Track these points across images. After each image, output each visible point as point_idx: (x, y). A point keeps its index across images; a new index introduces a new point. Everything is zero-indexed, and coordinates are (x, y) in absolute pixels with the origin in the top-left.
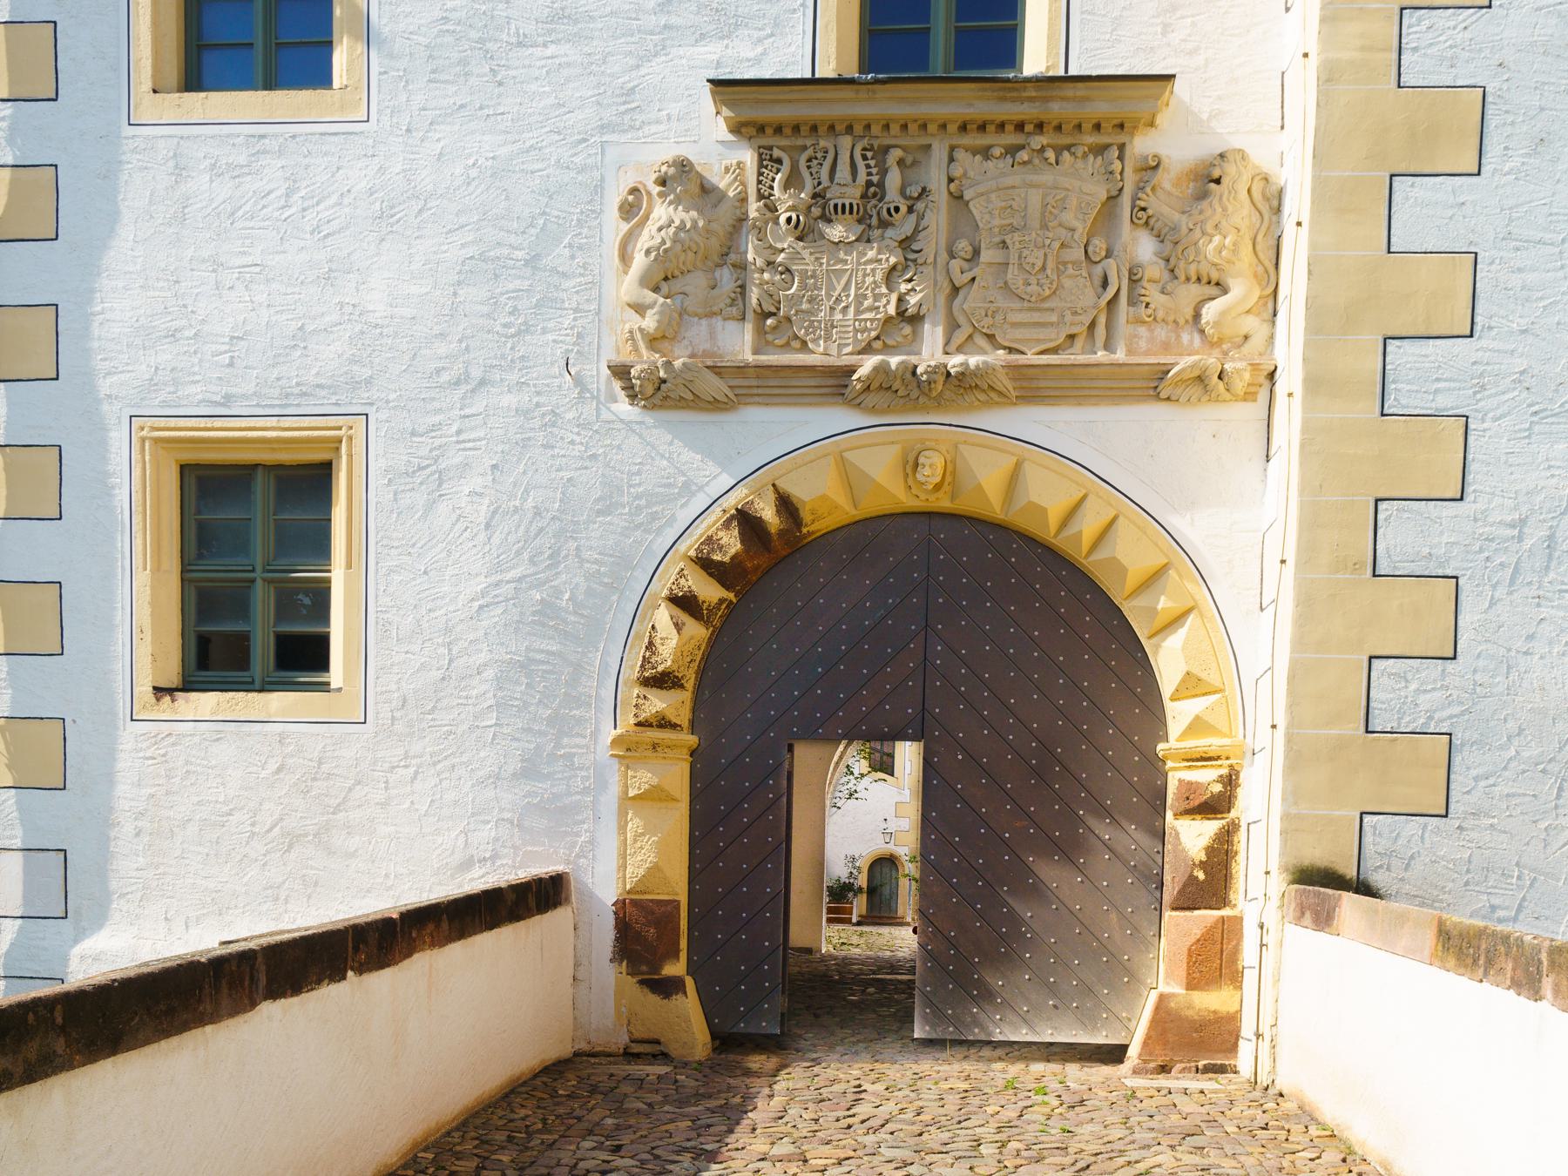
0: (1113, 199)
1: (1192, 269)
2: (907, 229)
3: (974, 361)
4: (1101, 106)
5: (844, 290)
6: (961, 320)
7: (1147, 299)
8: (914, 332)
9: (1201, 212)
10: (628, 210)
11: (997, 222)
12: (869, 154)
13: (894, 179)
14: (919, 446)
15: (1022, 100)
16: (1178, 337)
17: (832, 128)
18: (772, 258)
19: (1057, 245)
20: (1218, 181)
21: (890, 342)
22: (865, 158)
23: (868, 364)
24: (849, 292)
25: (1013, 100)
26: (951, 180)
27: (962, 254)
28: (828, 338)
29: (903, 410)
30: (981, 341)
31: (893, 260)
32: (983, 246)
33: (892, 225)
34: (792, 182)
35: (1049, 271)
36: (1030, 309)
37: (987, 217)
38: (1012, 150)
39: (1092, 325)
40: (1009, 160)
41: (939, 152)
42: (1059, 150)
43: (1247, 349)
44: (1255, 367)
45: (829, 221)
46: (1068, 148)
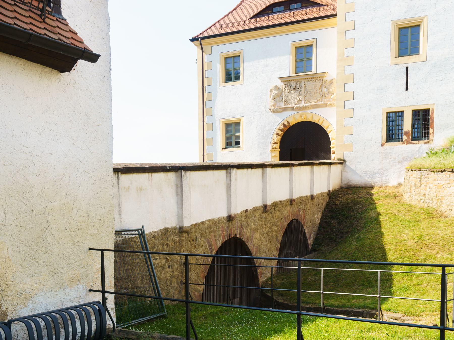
0: (322, 85)
10: (271, 91)
13: (298, 85)
34: (288, 87)
38: (311, 81)
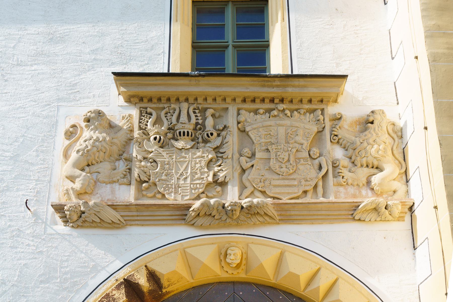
0: (320, 132)
1: (364, 161)
2: (218, 142)
3: (255, 201)
4: (312, 90)
5: (184, 170)
6: (247, 184)
7: (343, 174)
8: (223, 191)
9: (365, 136)
11: (263, 140)
12: (197, 111)
13: (210, 122)
14: (227, 245)
15: (273, 87)
16: (360, 192)
17: (178, 99)
18: (146, 156)
19: (294, 150)
20: (372, 123)
21: (210, 195)
22: (194, 112)
23: (197, 204)
24: (187, 174)
25: (269, 86)
26: (239, 123)
27: (246, 154)
28: (176, 193)
29: (219, 227)
30: (257, 193)
31: (210, 156)
32: (256, 150)
33: (210, 141)
34: (158, 121)
35: (291, 162)
36: (284, 179)
37: (258, 138)
38: (269, 111)
39: (316, 187)
40: (267, 115)
41: (232, 110)
42: (292, 111)
43: (396, 196)
44: (403, 204)
45: (177, 140)
46: (297, 110)
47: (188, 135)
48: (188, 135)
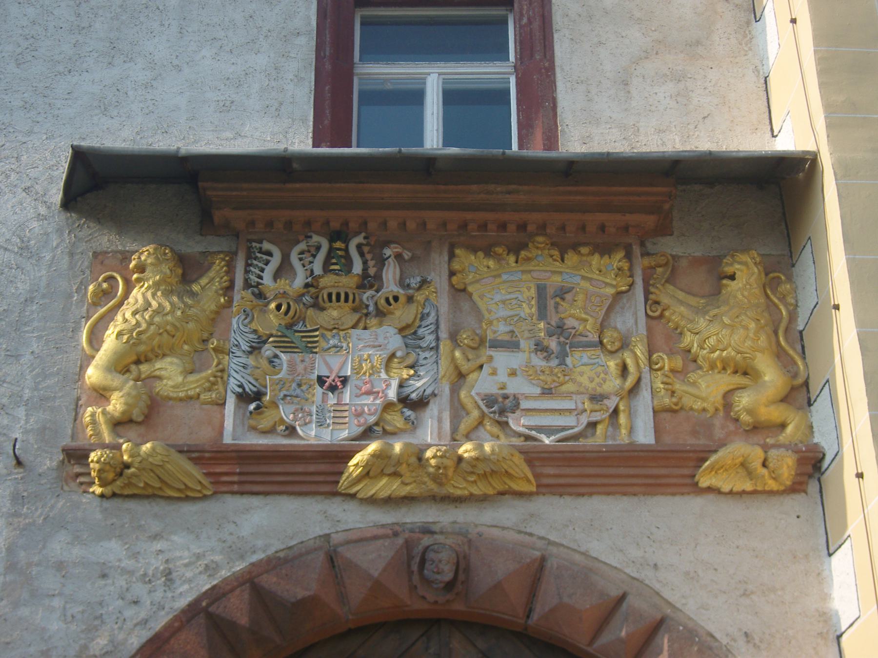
26: (452, 274)
28: (320, 424)
47: (346, 300)
48: (346, 300)
